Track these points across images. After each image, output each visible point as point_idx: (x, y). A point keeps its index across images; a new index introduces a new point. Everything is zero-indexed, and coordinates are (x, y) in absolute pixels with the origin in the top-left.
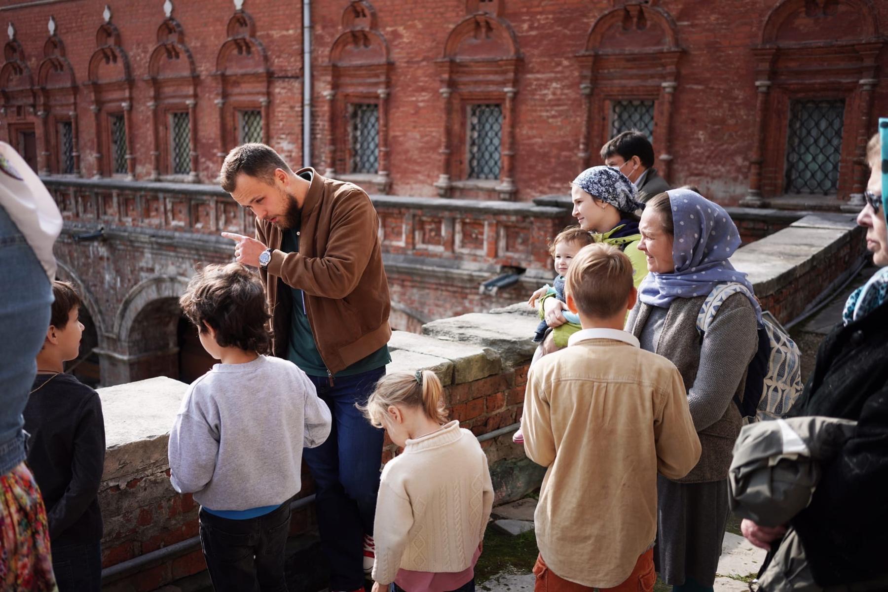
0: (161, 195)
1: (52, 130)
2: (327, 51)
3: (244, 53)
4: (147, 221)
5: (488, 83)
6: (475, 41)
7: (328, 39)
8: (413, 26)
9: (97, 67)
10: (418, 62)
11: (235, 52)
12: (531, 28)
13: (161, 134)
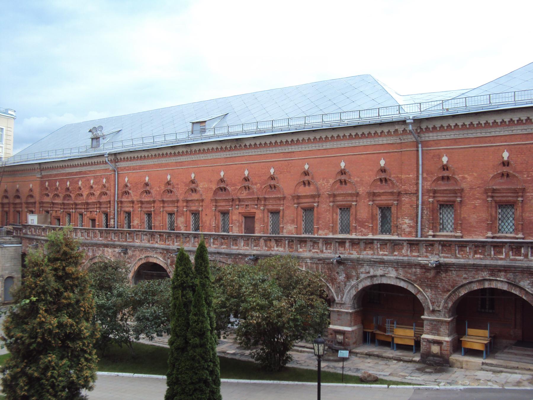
0: (375, 242)
1: (266, 215)
2: (429, 183)
3: (384, 183)
4: (365, 252)
5: (508, 197)
6: (501, 181)
7: (429, 179)
8: (473, 175)
9: (298, 188)
10: (475, 188)
11: (379, 183)
12: (528, 177)
13: (334, 217)
